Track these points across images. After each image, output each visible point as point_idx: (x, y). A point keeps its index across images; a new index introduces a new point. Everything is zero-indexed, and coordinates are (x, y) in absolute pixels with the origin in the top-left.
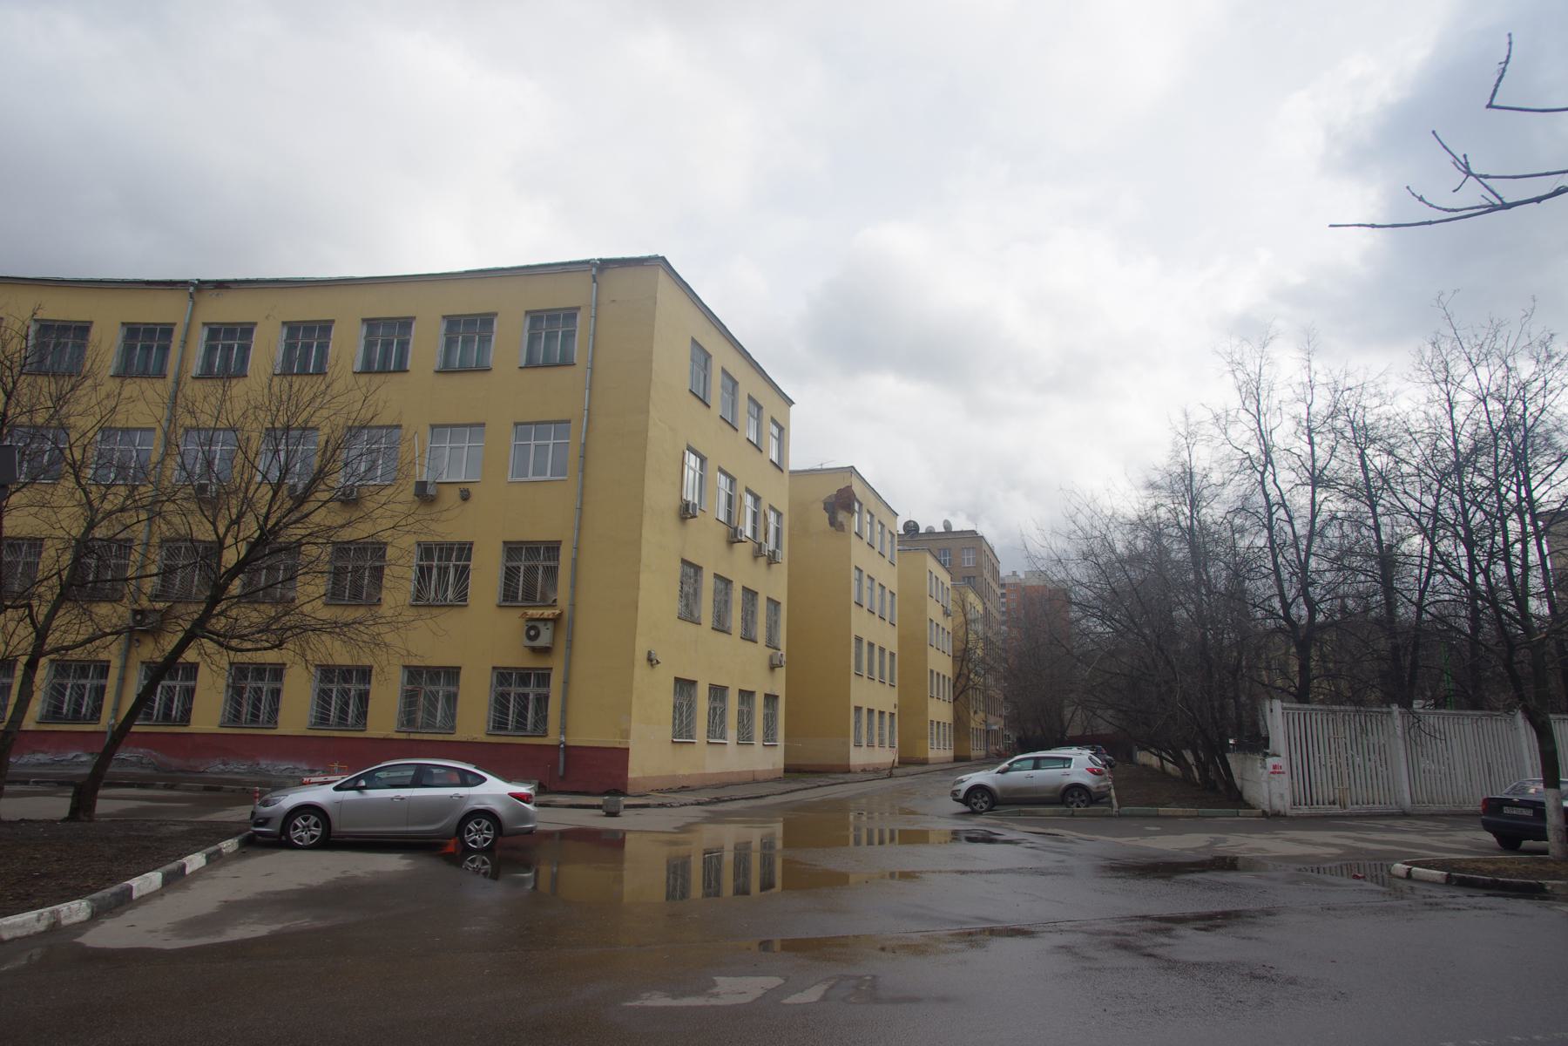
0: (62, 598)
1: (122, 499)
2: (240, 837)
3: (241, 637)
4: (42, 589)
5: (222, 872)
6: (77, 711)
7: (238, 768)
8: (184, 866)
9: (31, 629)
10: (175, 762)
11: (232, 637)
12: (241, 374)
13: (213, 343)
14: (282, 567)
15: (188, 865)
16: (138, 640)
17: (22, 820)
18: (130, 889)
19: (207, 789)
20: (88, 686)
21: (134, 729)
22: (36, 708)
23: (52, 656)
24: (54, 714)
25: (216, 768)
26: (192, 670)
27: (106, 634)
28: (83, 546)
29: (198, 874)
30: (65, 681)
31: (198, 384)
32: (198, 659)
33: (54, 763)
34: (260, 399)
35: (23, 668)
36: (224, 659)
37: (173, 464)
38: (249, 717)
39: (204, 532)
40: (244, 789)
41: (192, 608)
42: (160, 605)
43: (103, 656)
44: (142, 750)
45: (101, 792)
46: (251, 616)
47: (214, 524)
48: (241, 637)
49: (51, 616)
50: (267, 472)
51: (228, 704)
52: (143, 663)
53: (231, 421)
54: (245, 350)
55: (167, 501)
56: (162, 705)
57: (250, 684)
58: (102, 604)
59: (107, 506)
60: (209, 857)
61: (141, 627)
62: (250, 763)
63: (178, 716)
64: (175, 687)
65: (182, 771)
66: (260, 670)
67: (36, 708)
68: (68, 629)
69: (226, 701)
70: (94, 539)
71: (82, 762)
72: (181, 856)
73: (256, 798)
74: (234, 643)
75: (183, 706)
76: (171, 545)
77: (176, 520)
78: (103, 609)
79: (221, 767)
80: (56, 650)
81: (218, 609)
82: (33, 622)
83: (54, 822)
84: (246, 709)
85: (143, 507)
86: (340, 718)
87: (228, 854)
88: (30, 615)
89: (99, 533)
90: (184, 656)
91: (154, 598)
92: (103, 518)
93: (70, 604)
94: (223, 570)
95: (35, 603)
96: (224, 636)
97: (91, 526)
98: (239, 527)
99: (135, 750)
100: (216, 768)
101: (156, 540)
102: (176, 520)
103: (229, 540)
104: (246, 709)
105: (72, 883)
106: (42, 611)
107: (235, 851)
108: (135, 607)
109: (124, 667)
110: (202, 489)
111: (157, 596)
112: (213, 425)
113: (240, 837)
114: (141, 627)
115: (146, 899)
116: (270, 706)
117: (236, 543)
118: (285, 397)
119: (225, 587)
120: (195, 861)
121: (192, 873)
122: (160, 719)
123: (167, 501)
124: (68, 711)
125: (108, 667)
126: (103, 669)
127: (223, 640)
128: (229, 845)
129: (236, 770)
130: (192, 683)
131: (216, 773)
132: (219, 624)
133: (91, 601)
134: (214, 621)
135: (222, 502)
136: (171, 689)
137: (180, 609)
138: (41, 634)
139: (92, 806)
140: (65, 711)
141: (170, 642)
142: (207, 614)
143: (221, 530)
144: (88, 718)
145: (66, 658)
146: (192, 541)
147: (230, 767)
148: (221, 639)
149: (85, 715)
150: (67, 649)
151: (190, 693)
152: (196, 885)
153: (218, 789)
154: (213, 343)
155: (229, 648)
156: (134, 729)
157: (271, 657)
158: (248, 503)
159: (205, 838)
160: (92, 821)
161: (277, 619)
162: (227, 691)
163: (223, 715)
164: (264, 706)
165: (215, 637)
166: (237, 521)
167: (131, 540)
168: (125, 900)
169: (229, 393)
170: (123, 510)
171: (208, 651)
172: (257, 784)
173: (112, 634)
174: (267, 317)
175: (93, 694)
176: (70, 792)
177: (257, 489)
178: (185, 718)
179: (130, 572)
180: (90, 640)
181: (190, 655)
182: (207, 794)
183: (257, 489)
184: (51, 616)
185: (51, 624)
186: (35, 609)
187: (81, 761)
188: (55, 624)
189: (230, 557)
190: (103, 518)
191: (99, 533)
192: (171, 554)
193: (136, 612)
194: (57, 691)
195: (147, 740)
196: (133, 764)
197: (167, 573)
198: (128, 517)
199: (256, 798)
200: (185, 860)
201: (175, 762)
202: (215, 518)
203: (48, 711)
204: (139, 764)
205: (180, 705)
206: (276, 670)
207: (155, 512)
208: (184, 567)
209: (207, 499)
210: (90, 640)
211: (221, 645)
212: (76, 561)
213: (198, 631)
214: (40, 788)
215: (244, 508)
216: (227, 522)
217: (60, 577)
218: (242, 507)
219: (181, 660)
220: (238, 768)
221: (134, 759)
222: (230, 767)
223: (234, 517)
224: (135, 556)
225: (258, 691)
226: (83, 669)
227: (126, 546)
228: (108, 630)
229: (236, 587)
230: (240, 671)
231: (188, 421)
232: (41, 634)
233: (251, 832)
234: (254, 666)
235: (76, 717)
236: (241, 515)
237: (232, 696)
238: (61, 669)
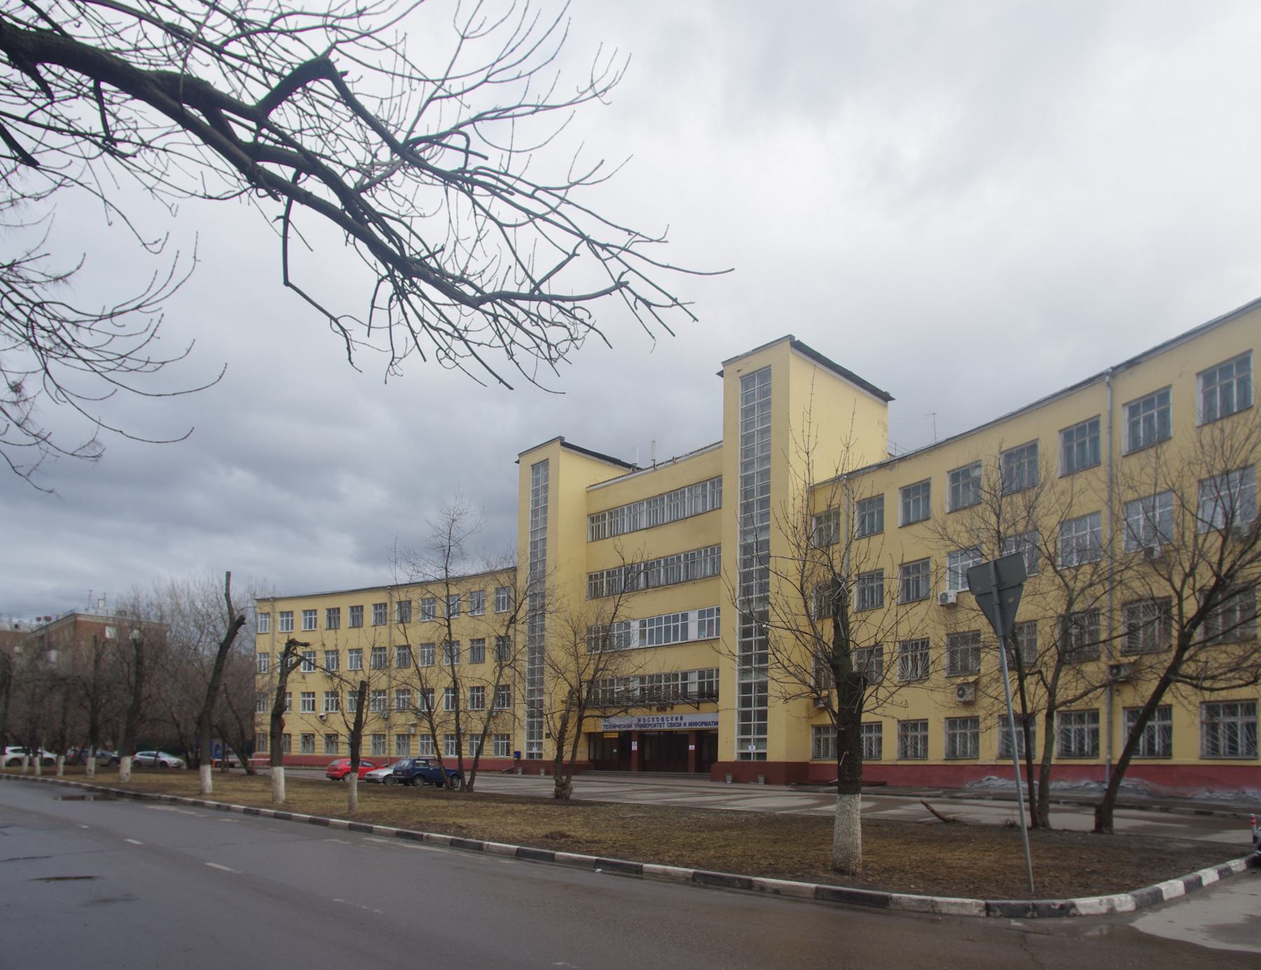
0: (1061, 663)
1: (1089, 576)
2: (1246, 858)
3: (1213, 678)
4: (1046, 659)
5: (1238, 888)
6: (1081, 749)
7: (1223, 796)
8: (1200, 879)
9: (1045, 689)
10: (1164, 790)
11: (1205, 679)
12: (1165, 438)
13: (1135, 419)
14: (1238, 608)
15: (1203, 878)
16: (1118, 690)
17: (1065, 830)
18: (1160, 892)
19: (1198, 813)
20: (1086, 730)
21: (1132, 762)
22: (1056, 749)
23: (1062, 708)
24: (1066, 752)
25: (1202, 795)
26: (1167, 712)
27: (1096, 688)
28: (1066, 620)
29: (1213, 886)
30: (1069, 727)
31: (1134, 461)
32: (1174, 702)
33: (1073, 789)
34: (1193, 454)
35: (1044, 717)
36: (1195, 697)
37: (1122, 538)
38: (1227, 750)
39: (1161, 589)
40: (1235, 815)
41: (1163, 657)
42: (1132, 659)
43: (1096, 705)
44: (1135, 779)
45: (1116, 812)
46: (1218, 657)
47: (1170, 580)
48: (1213, 678)
49: (1056, 677)
50: (1212, 522)
51: (1205, 739)
52: (1124, 708)
53: (1170, 483)
54: (1164, 415)
55: (1125, 569)
56: (1146, 743)
57: (1224, 719)
58: (1090, 664)
59: (1079, 585)
60: (1220, 873)
61: (1117, 681)
62: (1235, 791)
63: (1161, 750)
64: (1154, 727)
65: (1172, 797)
66: (1231, 707)
67: (1056, 749)
68: (1069, 687)
69: (1202, 736)
70: (1074, 613)
71: (1092, 788)
72: (1194, 869)
73: (1253, 823)
74: (1207, 684)
75: (1164, 742)
76: (1130, 607)
77: (1136, 585)
78: (1089, 668)
79: (1207, 794)
80: (1064, 703)
81: (1186, 655)
82: (1045, 684)
83: (1085, 833)
84: (1223, 743)
85: (1106, 579)
86: (1230, 747)
87: (1238, 873)
88: (1042, 679)
89: (1077, 607)
90: (1163, 699)
91: (1124, 653)
92: (1079, 595)
93: (1067, 667)
94: (1185, 621)
95: (1043, 669)
96: (1197, 678)
97: (1070, 603)
98: (1194, 578)
99: (1130, 779)
100: (1202, 795)
101: (1118, 607)
102: (1136, 585)
103: (1187, 592)
104: (1223, 743)
105: (1115, 880)
106: (1049, 677)
107: (1244, 871)
108: (1112, 662)
109: (1110, 714)
110: (1149, 551)
111: (1126, 652)
112: (1153, 492)
113: (1246, 858)
114: (1117, 681)
115: (1174, 901)
116: (1248, 739)
117: (1194, 593)
118: (1217, 444)
119: (1190, 636)
120: (1209, 875)
121: (1209, 885)
122: (1146, 752)
123: (1125, 569)
124: (1075, 749)
125: (1098, 713)
126: (1095, 716)
127: (1196, 682)
128: (1237, 865)
129: (1222, 798)
130: (1167, 723)
131: (1205, 800)
132: (1189, 668)
133: (1081, 662)
134: (1184, 666)
135: (1173, 559)
136: (1151, 728)
137: (1148, 660)
138: (1052, 692)
139: (1109, 824)
140: (1073, 749)
141: (1149, 688)
142: (1178, 660)
143: (1178, 585)
144: (1090, 753)
145: (1072, 709)
146: (1153, 598)
147: (1216, 794)
148: (1194, 682)
149: (1159, 752)
150: (1071, 702)
151: (1167, 731)
152: (1216, 896)
153: (1210, 814)
154: (1135, 419)
155: (1202, 688)
156: (1132, 762)
157: (1246, 693)
158: (1199, 554)
159: (1211, 856)
160: (1112, 834)
161: (1245, 659)
162: (1202, 727)
163: (1202, 749)
164: (1241, 740)
165: (1189, 680)
166: (1191, 573)
167: (1098, 609)
168: (1157, 901)
169: (1162, 458)
170: (1091, 585)
171: (1184, 694)
172: (1250, 811)
173: (1101, 687)
174: (1180, 376)
175: (1091, 735)
176: (1093, 811)
177: (1205, 540)
178: (1167, 751)
179: (1103, 636)
180: (1085, 694)
181: (1167, 699)
182: (1201, 818)
183: (1205, 540)
184: (1056, 677)
185: (1056, 684)
186: (1045, 674)
187: (1093, 789)
188: (1060, 682)
189: (1191, 607)
190: (1079, 595)
191: (1077, 607)
192: (1132, 613)
193: (1112, 667)
194: (1066, 735)
195: (1140, 771)
196: (1129, 790)
197: (1132, 631)
198: (1099, 590)
199: (1253, 823)
200: (1201, 873)
201: (1164, 790)
202: (1170, 575)
203: (1062, 750)
204: (1135, 790)
205: (1161, 741)
206: (1248, 706)
207: (1112, 580)
208: (1147, 624)
209: (1157, 562)
210: (1085, 694)
211: (1196, 686)
212: (1065, 633)
213: (1172, 677)
214: (1067, 807)
215: (1196, 560)
216: (1181, 577)
217: (1057, 647)
218: (1193, 561)
219: (1161, 703)
220: (1223, 796)
221: (1130, 786)
222: (1216, 794)
223: (1187, 570)
224: (1103, 621)
225: (1081, 731)
226: (1080, 717)
227: (1093, 614)
228: (1098, 685)
229: (1198, 634)
230: (1212, 709)
231: (1130, 495)
232: (1052, 692)
233: (1256, 855)
234: (1225, 703)
235: (1081, 754)
236: (1193, 568)
237: (1207, 732)
238: (1066, 717)
